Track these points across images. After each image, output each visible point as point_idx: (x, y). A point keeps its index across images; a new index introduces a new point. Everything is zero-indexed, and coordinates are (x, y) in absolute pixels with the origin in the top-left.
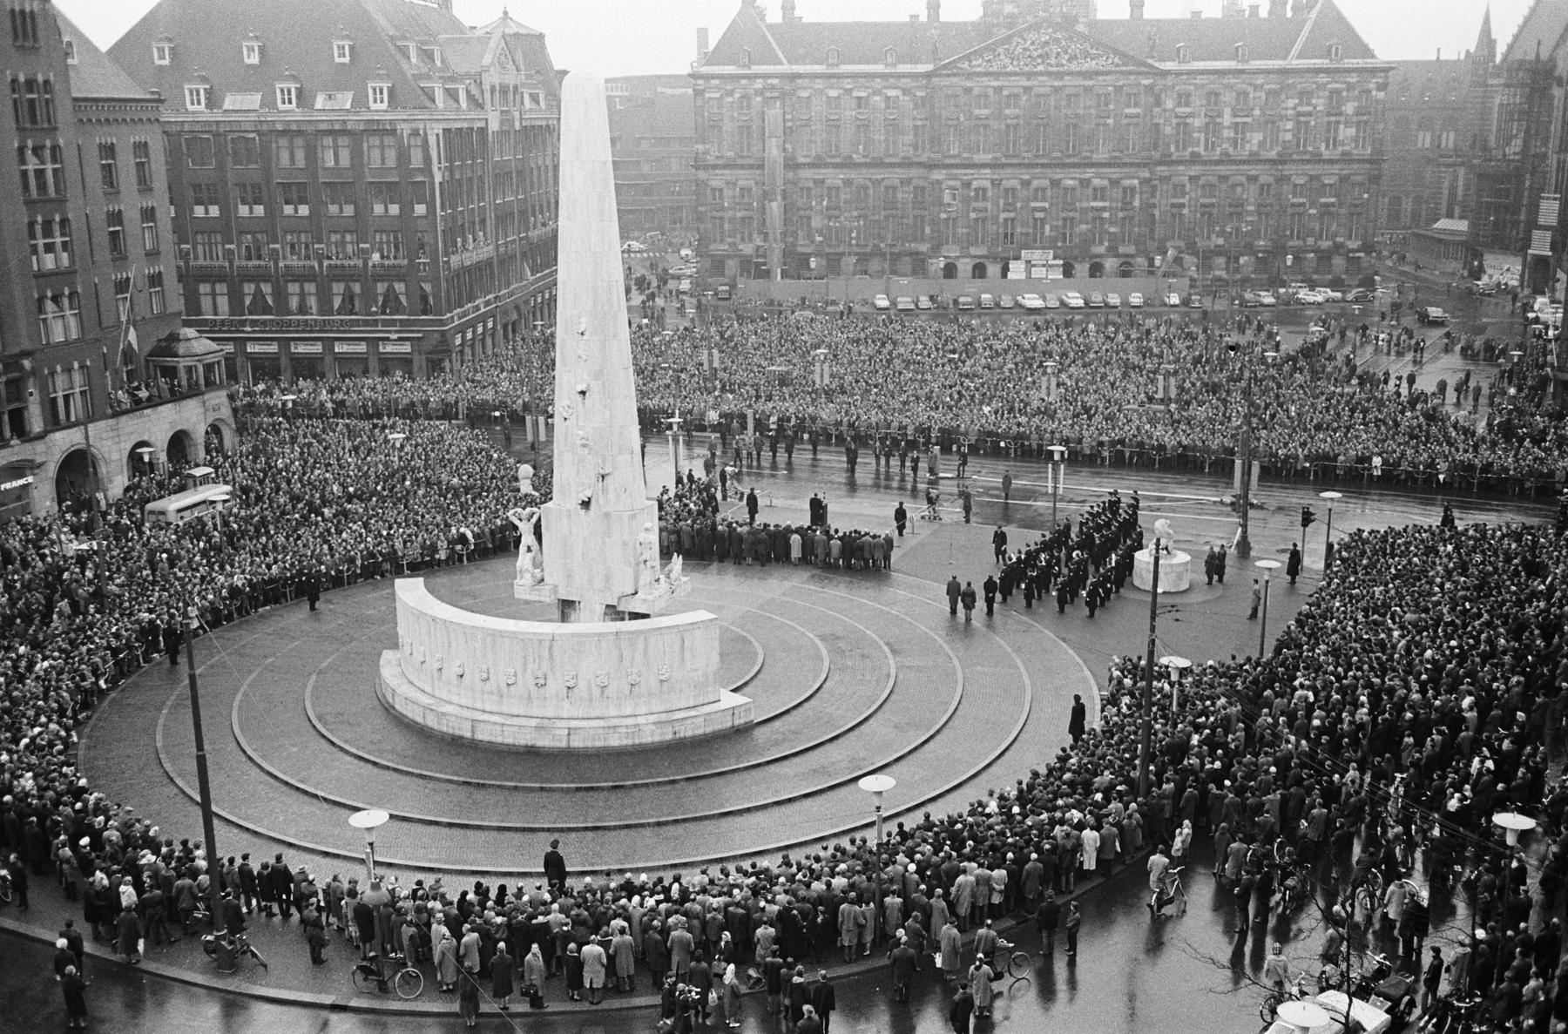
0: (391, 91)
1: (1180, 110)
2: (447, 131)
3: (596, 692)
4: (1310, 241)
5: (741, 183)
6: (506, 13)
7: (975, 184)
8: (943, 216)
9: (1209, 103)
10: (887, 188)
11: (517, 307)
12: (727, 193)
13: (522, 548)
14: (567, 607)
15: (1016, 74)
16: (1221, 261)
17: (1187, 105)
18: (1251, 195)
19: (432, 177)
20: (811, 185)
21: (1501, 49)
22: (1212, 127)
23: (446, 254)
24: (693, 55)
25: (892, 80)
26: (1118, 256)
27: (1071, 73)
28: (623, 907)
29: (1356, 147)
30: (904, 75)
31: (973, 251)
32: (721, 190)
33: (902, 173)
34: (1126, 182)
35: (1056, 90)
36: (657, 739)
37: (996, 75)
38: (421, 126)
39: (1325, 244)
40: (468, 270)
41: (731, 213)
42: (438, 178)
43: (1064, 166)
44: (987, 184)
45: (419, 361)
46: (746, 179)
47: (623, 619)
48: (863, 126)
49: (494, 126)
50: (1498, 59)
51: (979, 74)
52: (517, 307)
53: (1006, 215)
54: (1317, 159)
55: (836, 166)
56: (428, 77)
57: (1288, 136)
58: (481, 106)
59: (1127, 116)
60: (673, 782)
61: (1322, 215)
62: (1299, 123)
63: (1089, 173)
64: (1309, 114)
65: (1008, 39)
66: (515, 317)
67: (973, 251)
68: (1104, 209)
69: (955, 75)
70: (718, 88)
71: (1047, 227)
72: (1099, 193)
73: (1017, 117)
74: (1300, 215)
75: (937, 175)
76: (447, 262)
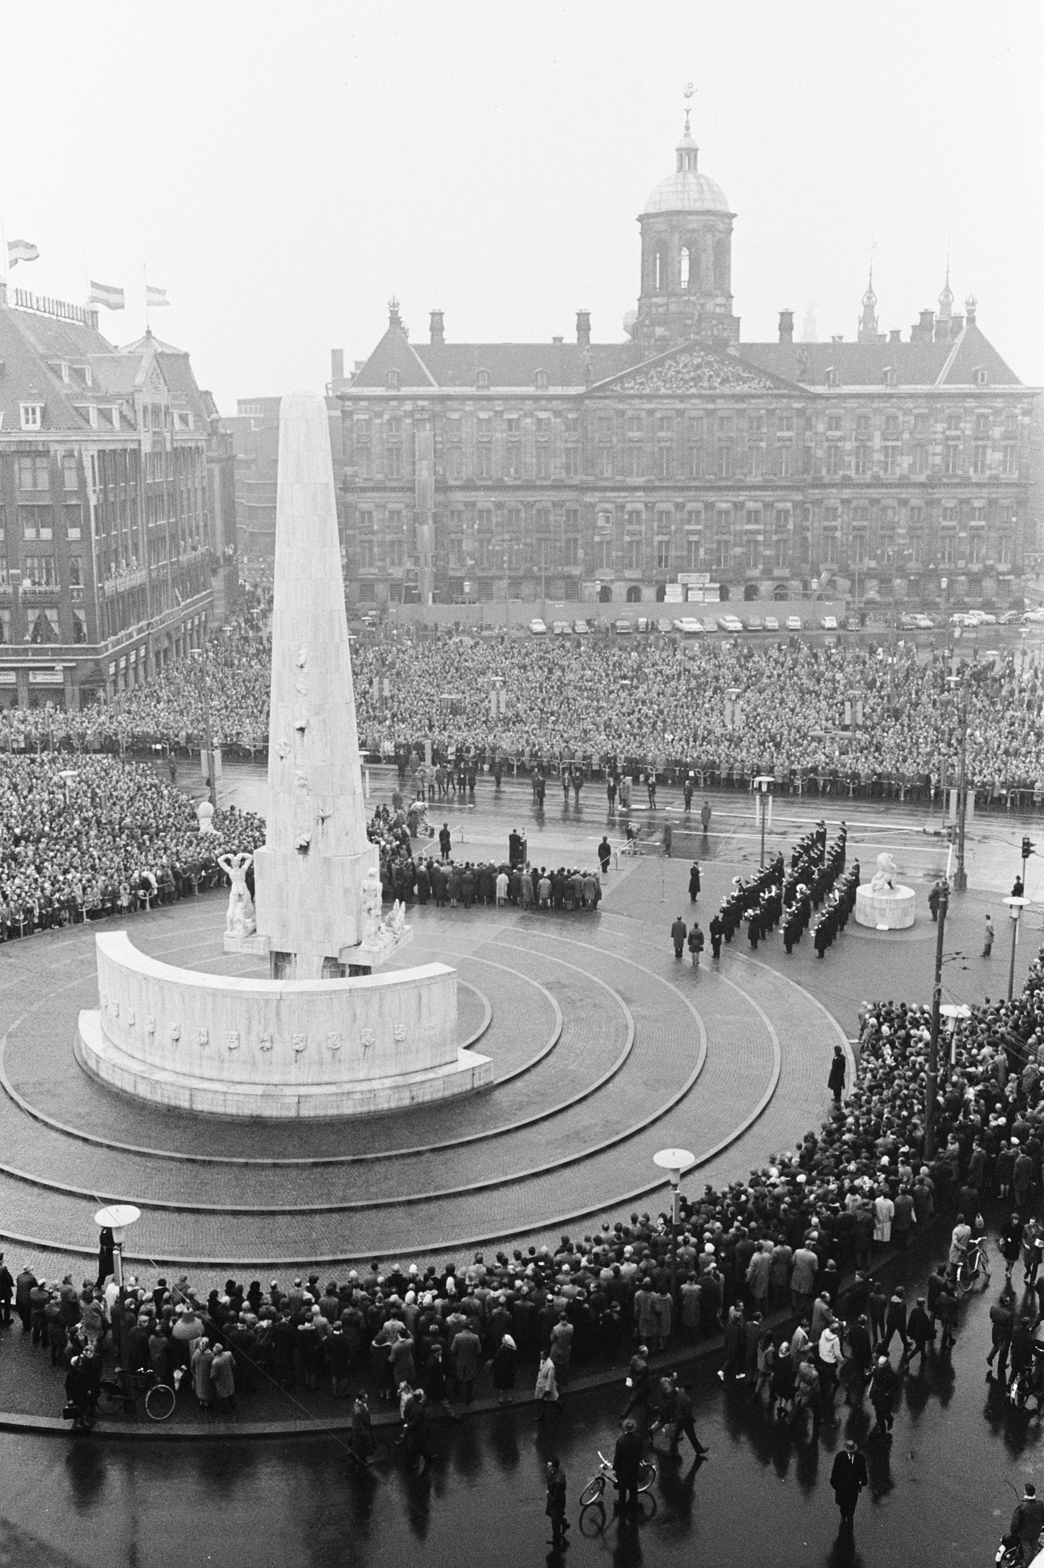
0: (44, 412)
2: (101, 452)
3: (327, 1055)
4: (961, 564)
5: (391, 506)
6: (149, 332)
7: (629, 507)
8: (597, 539)
9: (858, 428)
10: (539, 511)
11: (169, 635)
13: (233, 896)
14: (280, 960)
15: (669, 397)
16: (874, 583)
17: (837, 428)
18: (902, 517)
19: (87, 500)
20: (461, 507)
22: (863, 449)
23: (100, 580)
24: (328, 377)
25: (543, 402)
26: (773, 579)
27: (723, 396)
28: (394, 1305)
30: (558, 398)
31: (628, 574)
32: (370, 513)
33: (551, 496)
34: (780, 505)
35: (710, 413)
36: (393, 1105)
37: (649, 398)
38: (76, 447)
39: (976, 567)
40: (121, 596)
41: (380, 537)
42: (93, 501)
43: (720, 489)
44: (641, 507)
45: (72, 692)
46: (395, 502)
47: (343, 975)
48: (514, 448)
49: (146, 448)
51: (632, 397)
52: (169, 635)
53: (660, 538)
55: (487, 488)
56: (81, 396)
57: (938, 460)
58: (133, 427)
59: (779, 439)
60: (419, 1153)
61: (973, 538)
62: (948, 447)
63: (743, 496)
64: (958, 438)
65: (660, 363)
66: (166, 644)
68: (758, 532)
69: (607, 397)
70: (367, 409)
71: (702, 551)
72: (753, 516)
73: (671, 440)
74: (951, 537)
75: (590, 498)
76: (102, 588)
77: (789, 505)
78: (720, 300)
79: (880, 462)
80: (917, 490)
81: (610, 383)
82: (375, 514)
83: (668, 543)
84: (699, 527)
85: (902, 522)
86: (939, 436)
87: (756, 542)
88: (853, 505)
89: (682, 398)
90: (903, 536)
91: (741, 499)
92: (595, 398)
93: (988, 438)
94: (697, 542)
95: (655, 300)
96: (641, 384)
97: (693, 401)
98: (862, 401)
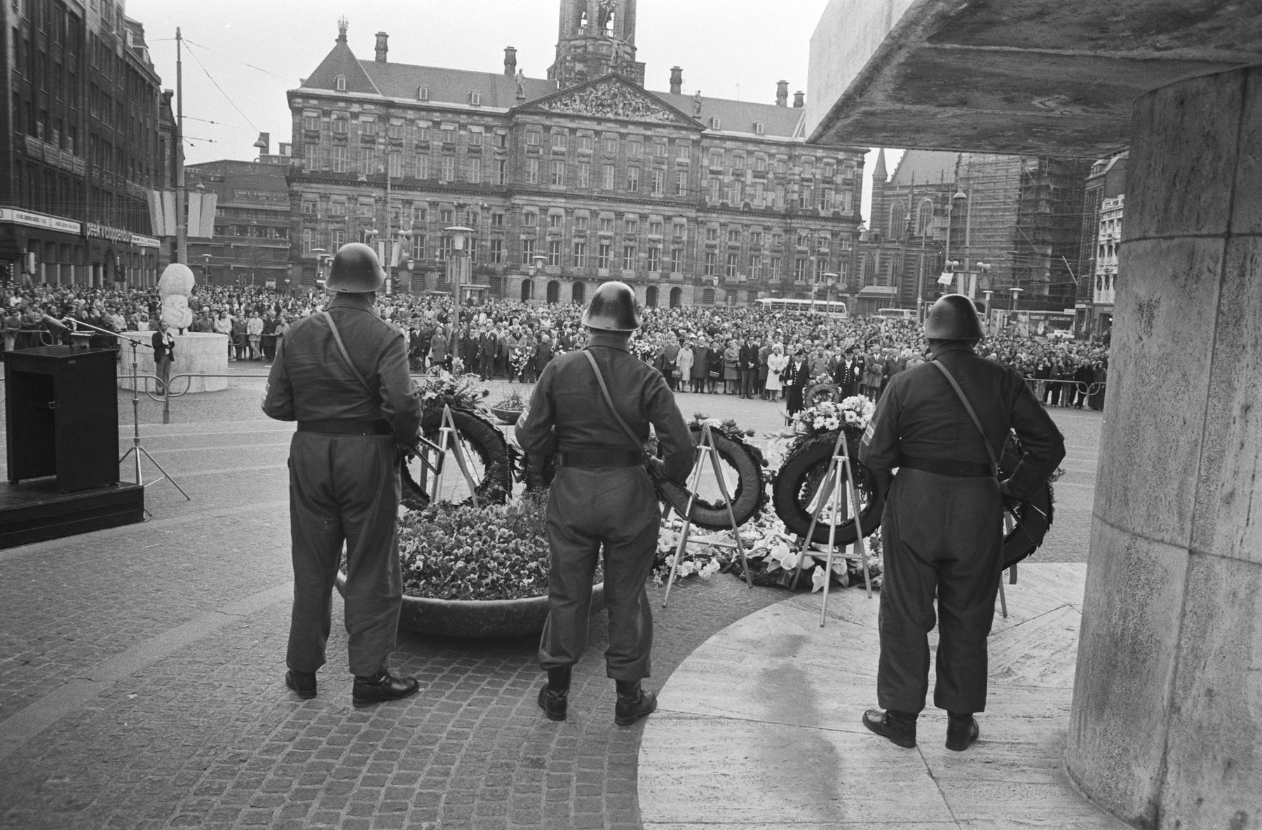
7: (552, 211)
8: (523, 237)
12: (321, 205)
18: (767, 241)
21: (891, 171)
25: (476, 118)
31: (548, 269)
34: (677, 220)
41: (323, 226)
44: (562, 212)
50: (889, 180)
54: (815, 216)
57: (795, 197)
59: (680, 165)
63: (647, 209)
67: (548, 269)
68: (658, 241)
69: (536, 114)
71: (611, 254)
77: (684, 220)
78: (628, 49)
81: (540, 101)
82: (319, 205)
83: (583, 245)
84: (611, 234)
85: (767, 246)
86: (797, 177)
87: (656, 249)
89: (600, 121)
90: (765, 257)
91: (646, 211)
93: (831, 182)
94: (607, 247)
95: (573, 43)
96: (566, 105)
97: (609, 125)
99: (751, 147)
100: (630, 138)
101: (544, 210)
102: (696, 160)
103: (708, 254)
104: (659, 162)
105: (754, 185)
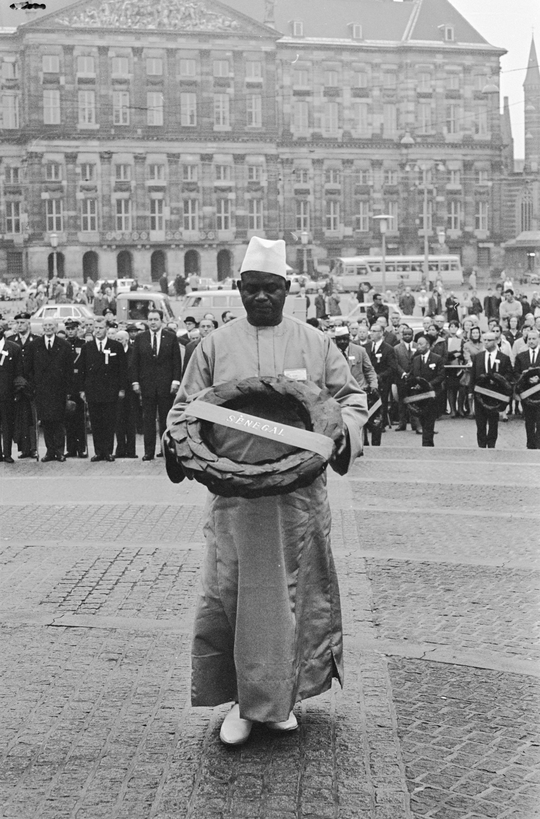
1: (296, 88)
29: (477, 131)
37: (101, 32)
44: (95, 159)
51: (83, 31)
54: (440, 143)
57: (411, 118)
59: (250, 85)
63: (210, 147)
64: (428, 96)
69: (52, 31)
71: (166, 211)
77: (262, 159)
79: (351, 120)
80: (390, 151)
83: (127, 201)
85: (377, 187)
87: (226, 201)
88: (325, 167)
89: (139, 34)
92: (38, 31)
93: (459, 97)
94: (160, 202)
96: (92, 17)
98: (331, 54)
99: (346, 57)
100: (181, 54)
101: (71, 158)
102: (271, 78)
103: (298, 202)
104: (222, 84)
105: (353, 106)
